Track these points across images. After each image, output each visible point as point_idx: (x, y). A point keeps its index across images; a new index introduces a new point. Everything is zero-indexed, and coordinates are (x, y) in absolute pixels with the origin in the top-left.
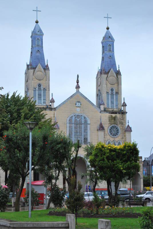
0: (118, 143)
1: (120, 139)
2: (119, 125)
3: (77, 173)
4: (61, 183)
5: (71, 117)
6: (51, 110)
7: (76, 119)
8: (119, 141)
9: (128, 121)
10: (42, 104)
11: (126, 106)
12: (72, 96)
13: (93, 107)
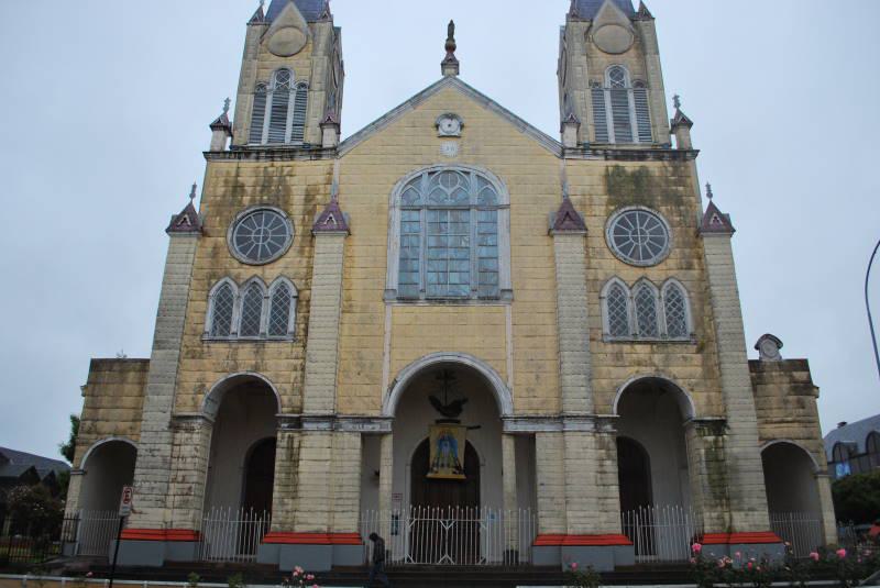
0: (663, 294)
1: (672, 273)
2: (663, 209)
3: (481, 461)
4: (350, 502)
5: (410, 183)
6: (319, 157)
7: (441, 186)
8: (668, 282)
9: (708, 186)
10: (288, 140)
11: (689, 124)
12: (417, 99)
13: (525, 133)
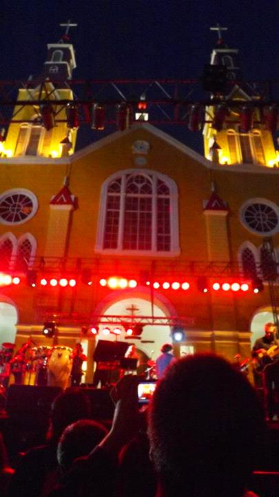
7: (134, 183)
